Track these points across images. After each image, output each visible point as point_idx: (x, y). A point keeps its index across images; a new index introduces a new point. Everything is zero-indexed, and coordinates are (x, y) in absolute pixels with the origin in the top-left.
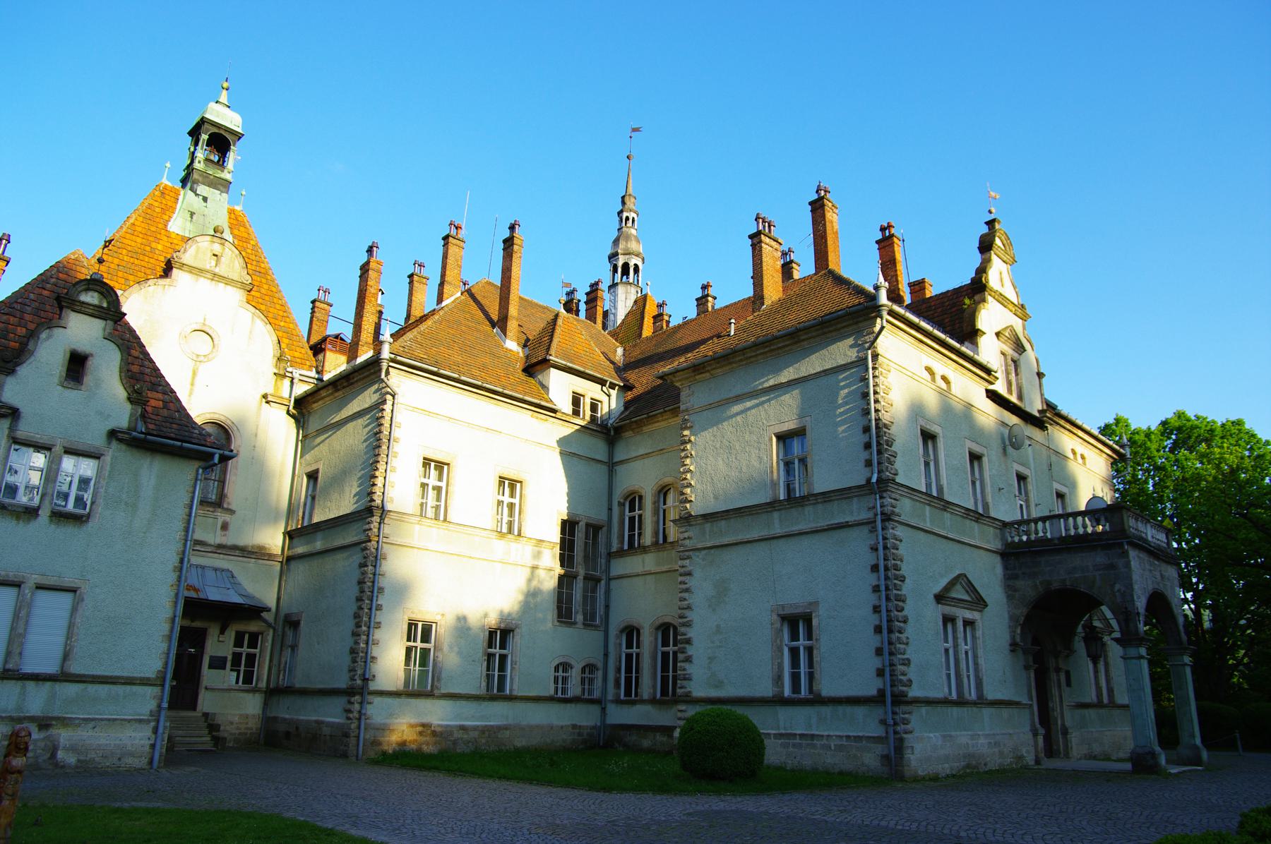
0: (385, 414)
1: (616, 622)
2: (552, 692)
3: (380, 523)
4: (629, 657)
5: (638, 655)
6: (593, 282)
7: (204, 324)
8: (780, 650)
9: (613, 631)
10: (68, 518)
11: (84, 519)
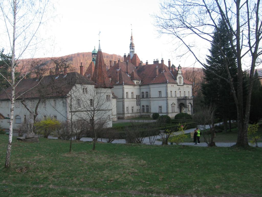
1: (142, 105)
9: (141, 106)
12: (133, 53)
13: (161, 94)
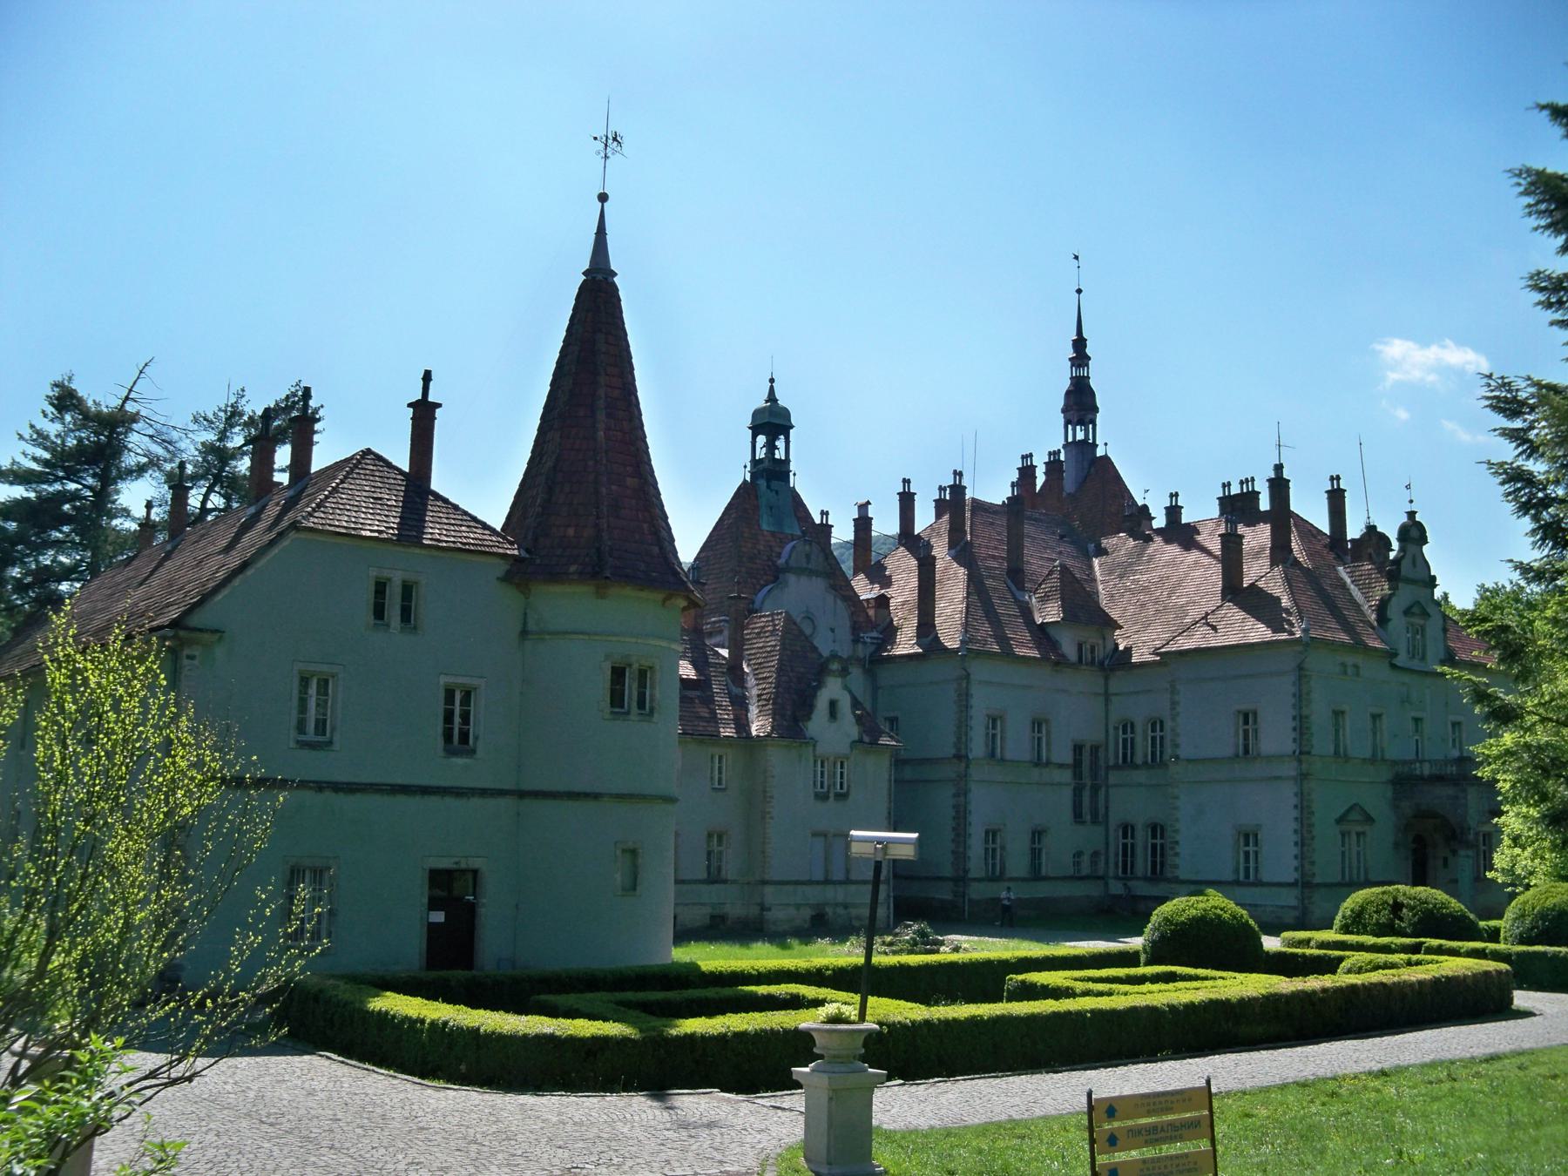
1: (1114, 820)
2: (1071, 872)
4: (1125, 846)
5: (1132, 845)
8: (1238, 853)
13: (1256, 731)
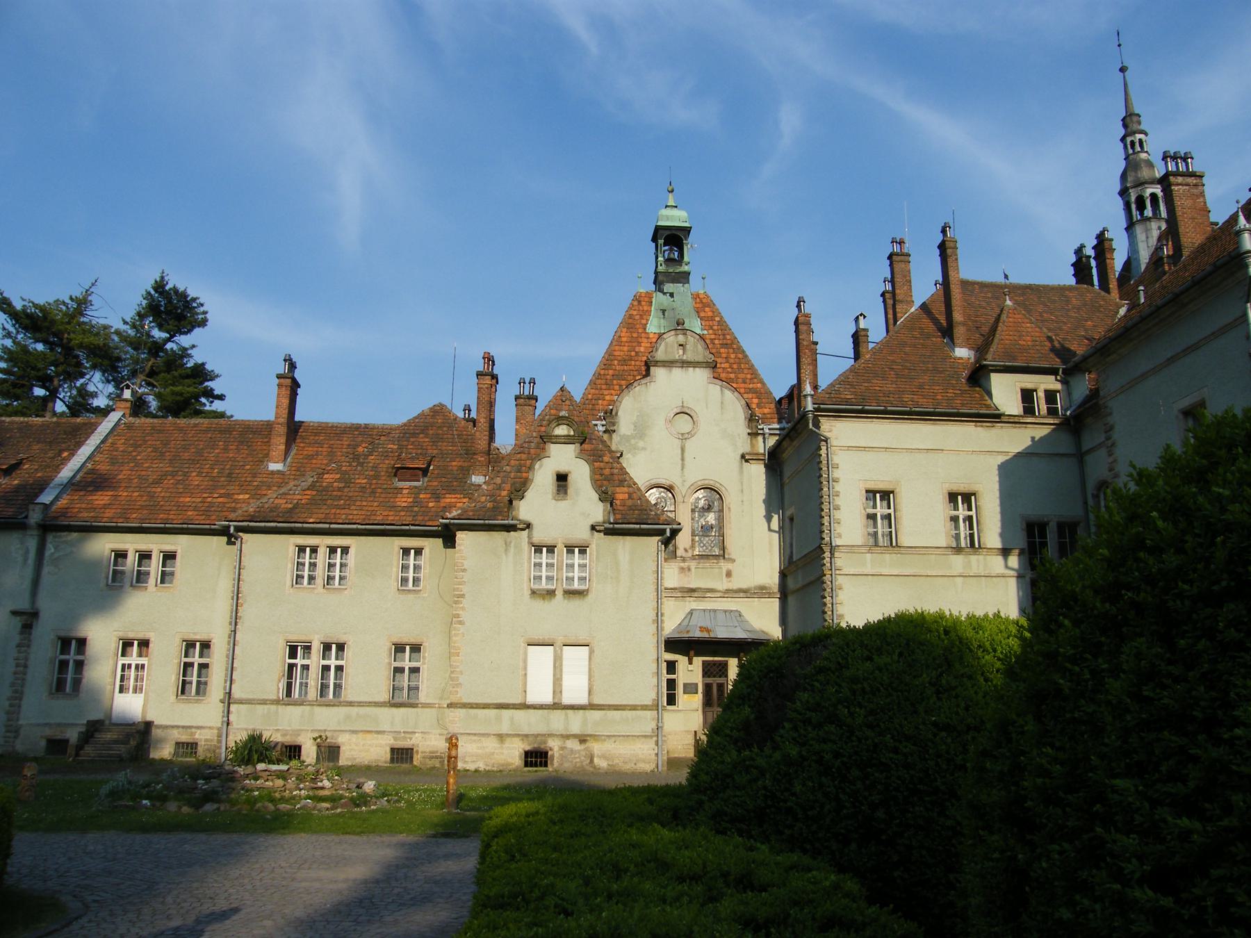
0: (822, 459)
3: (831, 558)
6: (1098, 233)
7: (683, 406)
10: (575, 594)
11: (585, 593)
12: (1147, 231)
